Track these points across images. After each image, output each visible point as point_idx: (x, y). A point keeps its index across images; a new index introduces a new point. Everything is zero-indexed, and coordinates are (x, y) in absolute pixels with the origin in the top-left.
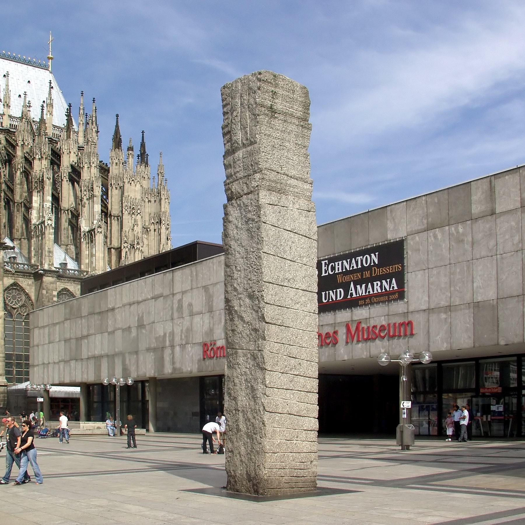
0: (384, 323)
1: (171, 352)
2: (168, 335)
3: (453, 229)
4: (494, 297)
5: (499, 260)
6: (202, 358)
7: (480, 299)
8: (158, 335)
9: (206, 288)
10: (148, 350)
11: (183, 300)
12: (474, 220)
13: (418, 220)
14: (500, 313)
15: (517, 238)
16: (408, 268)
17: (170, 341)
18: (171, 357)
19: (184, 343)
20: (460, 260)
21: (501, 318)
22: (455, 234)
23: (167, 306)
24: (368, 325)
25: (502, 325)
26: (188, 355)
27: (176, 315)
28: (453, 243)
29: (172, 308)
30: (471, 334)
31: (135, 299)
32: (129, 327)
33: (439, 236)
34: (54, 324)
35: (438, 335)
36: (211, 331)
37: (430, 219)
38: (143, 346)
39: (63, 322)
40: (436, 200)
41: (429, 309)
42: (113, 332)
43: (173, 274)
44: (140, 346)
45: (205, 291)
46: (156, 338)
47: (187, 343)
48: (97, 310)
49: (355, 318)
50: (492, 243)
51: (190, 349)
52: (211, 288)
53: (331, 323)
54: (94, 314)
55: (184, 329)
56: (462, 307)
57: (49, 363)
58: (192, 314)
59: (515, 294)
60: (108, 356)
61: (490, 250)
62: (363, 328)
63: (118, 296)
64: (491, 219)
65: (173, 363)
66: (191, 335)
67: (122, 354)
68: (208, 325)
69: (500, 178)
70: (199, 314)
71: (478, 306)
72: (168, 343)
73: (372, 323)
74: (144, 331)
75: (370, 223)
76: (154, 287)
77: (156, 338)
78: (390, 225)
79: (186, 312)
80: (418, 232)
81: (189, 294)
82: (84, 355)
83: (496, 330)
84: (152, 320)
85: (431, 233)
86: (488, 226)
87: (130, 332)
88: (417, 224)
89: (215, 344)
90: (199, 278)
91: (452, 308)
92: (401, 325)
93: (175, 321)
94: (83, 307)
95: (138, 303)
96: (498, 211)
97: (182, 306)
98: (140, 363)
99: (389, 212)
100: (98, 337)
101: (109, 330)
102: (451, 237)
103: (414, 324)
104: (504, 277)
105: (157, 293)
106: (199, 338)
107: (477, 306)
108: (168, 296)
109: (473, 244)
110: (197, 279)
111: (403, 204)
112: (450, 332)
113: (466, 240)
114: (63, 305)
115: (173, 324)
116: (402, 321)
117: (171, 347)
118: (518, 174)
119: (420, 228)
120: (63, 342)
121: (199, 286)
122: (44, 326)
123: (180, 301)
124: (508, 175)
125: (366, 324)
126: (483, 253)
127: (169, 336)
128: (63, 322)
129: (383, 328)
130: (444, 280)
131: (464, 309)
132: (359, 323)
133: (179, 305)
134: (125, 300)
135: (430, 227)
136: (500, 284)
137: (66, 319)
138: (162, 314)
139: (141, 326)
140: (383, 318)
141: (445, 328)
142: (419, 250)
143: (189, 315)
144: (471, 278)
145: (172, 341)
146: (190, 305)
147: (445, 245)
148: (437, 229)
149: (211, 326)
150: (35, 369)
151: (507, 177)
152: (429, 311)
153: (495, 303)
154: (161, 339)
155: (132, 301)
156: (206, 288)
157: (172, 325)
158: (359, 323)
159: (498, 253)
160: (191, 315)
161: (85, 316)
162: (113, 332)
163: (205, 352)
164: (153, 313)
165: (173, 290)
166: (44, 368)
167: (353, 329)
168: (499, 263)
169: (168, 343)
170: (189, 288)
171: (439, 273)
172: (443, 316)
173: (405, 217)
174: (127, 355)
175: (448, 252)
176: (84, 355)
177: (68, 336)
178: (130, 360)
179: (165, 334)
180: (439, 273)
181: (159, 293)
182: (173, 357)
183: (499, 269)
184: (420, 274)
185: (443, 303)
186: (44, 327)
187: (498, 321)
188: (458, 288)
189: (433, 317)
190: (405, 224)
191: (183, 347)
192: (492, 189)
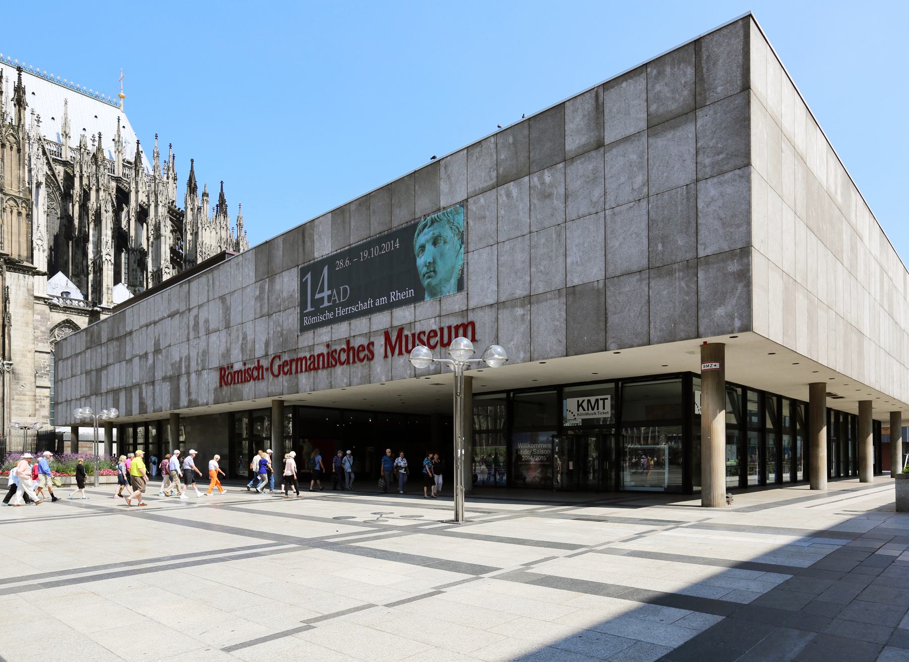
0: (434, 327)
1: (187, 381)
2: (184, 360)
3: (536, 179)
4: (601, 276)
5: (608, 217)
6: (218, 385)
7: (577, 281)
8: (174, 361)
9: (222, 298)
10: (164, 379)
12: (568, 160)
13: (483, 174)
14: (609, 301)
15: (639, 179)
16: (469, 245)
17: (185, 367)
18: (187, 387)
19: (200, 368)
20: (546, 224)
21: (611, 309)
22: (539, 187)
23: (183, 324)
24: (413, 332)
25: (613, 319)
26: (205, 384)
28: (535, 201)
29: (188, 328)
30: (562, 336)
31: (152, 319)
32: (146, 354)
34: (77, 355)
35: (511, 340)
37: (501, 170)
38: (159, 375)
39: (84, 351)
40: (511, 140)
41: (498, 303)
42: (131, 360)
45: (222, 302)
46: (172, 365)
47: (203, 369)
48: (116, 335)
49: (396, 323)
50: (597, 192)
51: (206, 376)
52: (228, 297)
54: (113, 339)
55: (201, 351)
56: (549, 296)
57: (72, 400)
58: (208, 333)
59: (635, 268)
61: (594, 204)
62: (407, 336)
63: (135, 317)
64: (597, 155)
65: (189, 394)
67: (138, 385)
68: (225, 344)
69: (612, 87)
71: (574, 293)
73: (418, 329)
74: (160, 357)
75: (416, 188)
77: (172, 365)
78: (444, 186)
80: (483, 191)
81: (205, 308)
82: (104, 390)
83: (603, 327)
85: (502, 190)
86: (591, 167)
87: (147, 359)
89: (232, 367)
90: (215, 287)
91: (533, 299)
93: (191, 342)
94: (103, 333)
95: (155, 323)
96: (607, 141)
97: (198, 323)
98: (156, 395)
99: (442, 169)
100: (117, 366)
101: (127, 358)
102: (532, 192)
103: (477, 326)
104: (617, 244)
105: (173, 309)
106: (215, 362)
107: (572, 293)
108: (183, 312)
110: (213, 287)
111: (462, 152)
113: (555, 193)
116: (459, 323)
118: (644, 75)
119: (485, 185)
120: (84, 375)
122: (67, 358)
123: (197, 317)
124: (626, 80)
125: (411, 331)
126: (583, 210)
127: (185, 361)
128: (84, 351)
130: (521, 257)
131: (551, 299)
132: (401, 330)
133: (195, 322)
134: (143, 322)
135: (501, 181)
136: (609, 256)
137: (87, 349)
139: (157, 351)
140: (433, 320)
141: (522, 329)
142: (484, 217)
143: (205, 334)
144: (562, 250)
145: (188, 367)
146: (207, 321)
147: (523, 206)
148: (512, 183)
149: (228, 346)
150: (59, 406)
151: (624, 84)
152: (498, 305)
153: (601, 285)
156: (222, 298)
158: (401, 330)
159: (607, 207)
161: (104, 343)
162: (131, 360)
163: (222, 378)
165: (189, 305)
166: (67, 405)
167: (394, 339)
168: (608, 222)
171: (513, 249)
172: (519, 311)
173: (465, 171)
174: (144, 386)
175: (527, 215)
176: (104, 390)
177: (88, 368)
178: (147, 391)
180: (513, 249)
182: (189, 386)
183: (608, 232)
184: (485, 253)
185: (520, 292)
186: (67, 358)
187: (606, 314)
188: (542, 268)
189: (505, 314)
190: (465, 183)
192: (599, 108)
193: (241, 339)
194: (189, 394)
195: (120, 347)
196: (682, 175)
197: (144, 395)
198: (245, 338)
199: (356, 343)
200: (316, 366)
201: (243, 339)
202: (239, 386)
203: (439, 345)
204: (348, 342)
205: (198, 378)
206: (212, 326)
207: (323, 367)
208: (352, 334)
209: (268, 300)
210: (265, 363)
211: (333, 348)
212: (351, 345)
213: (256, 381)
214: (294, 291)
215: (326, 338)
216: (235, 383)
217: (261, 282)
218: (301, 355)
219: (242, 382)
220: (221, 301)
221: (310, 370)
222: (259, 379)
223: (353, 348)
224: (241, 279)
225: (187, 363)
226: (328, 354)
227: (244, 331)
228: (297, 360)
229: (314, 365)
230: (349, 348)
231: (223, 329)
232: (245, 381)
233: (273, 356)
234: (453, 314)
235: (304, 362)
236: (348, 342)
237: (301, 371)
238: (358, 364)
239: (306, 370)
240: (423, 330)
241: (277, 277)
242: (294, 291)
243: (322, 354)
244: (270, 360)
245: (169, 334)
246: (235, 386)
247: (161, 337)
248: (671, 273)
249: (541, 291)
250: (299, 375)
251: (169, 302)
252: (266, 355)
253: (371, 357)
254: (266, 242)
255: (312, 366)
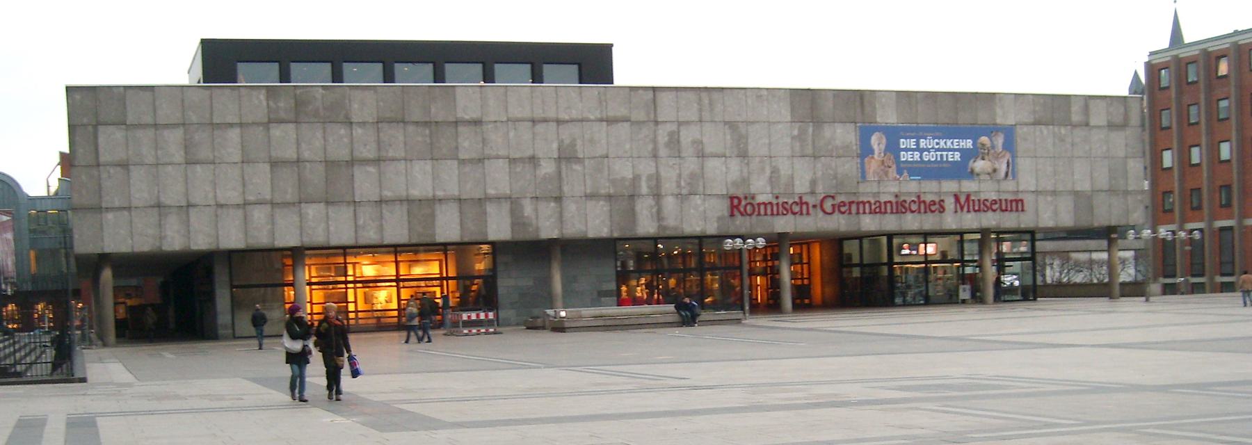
0: (994, 198)
4: (1089, 189)
6: (726, 213)
7: (1079, 189)
8: (618, 177)
9: (732, 125)
11: (681, 133)
12: (1074, 126)
15: (1105, 148)
17: (649, 187)
18: (654, 210)
19: (684, 192)
27: (663, 152)
29: (655, 141)
31: (551, 114)
32: (533, 160)
33: (1045, 132)
36: (745, 181)
37: (1037, 116)
43: (654, 96)
44: (566, 188)
45: (730, 127)
46: (613, 182)
49: (964, 190)
50: (1087, 148)
51: (699, 202)
53: (935, 191)
55: (686, 173)
60: (460, 200)
62: (973, 200)
65: (659, 216)
66: (701, 184)
70: (719, 157)
72: (644, 189)
73: (983, 197)
74: (577, 167)
76: (604, 104)
78: (999, 111)
79: (688, 150)
80: (1026, 124)
84: (600, 151)
85: (1038, 127)
88: (1026, 117)
89: (753, 198)
92: (1011, 201)
95: (559, 122)
96: (1092, 123)
97: (679, 142)
98: (567, 215)
101: (462, 156)
103: (1025, 201)
107: (1076, 194)
108: (639, 123)
109: (1073, 145)
110: (712, 110)
112: (1056, 213)
114: (264, 91)
115: (657, 165)
116: (1013, 198)
117: (654, 196)
119: (1027, 121)
121: (717, 120)
125: (975, 196)
129: (995, 202)
138: (628, 146)
139: (567, 156)
146: (698, 144)
149: (746, 175)
152: (1036, 192)
154: (627, 183)
155: (538, 114)
156: (732, 125)
157: (654, 165)
160: (701, 155)
164: (603, 141)
165: (655, 116)
167: (963, 199)
169: (644, 189)
170: (695, 118)
172: (1049, 199)
177: (291, 154)
179: (636, 179)
181: (619, 114)
182: (659, 212)
185: (1049, 188)
189: (1041, 198)
191: (680, 197)
193: (768, 171)
194: (659, 216)
195: (431, 136)
196: (1122, 154)
197: (528, 209)
198: (775, 171)
199: (928, 198)
200: (883, 210)
201: (772, 172)
202: (768, 218)
203: (999, 210)
204: (919, 197)
205: (682, 203)
206: (709, 149)
207: (892, 213)
208: (923, 191)
209: (814, 142)
210: (811, 200)
211: (902, 198)
212: (922, 199)
213: (797, 216)
214: (851, 142)
215: (895, 190)
216: (759, 214)
217: (801, 124)
218: (865, 200)
219: (772, 214)
220: (727, 127)
221: (876, 213)
222: (802, 214)
223: (924, 202)
224: (765, 113)
225: (654, 183)
226: (897, 203)
227: (774, 164)
228: (858, 203)
229: (880, 209)
230: (920, 202)
231: (733, 155)
232: (778, 214)
233: (823, 195)
234: (1008, 192)
235: (867, 205)
236: (919, 197)
237: (864, 213)
238: (929, 214)
239: (870, 213)
240: (986, 198)
241: (826, 127)
242: (851, 142)
243: (890, 202)
244: (821, 197)
245: (604, 142)
246: (760, 218)
247: (579, 142)
248: (1118, 195)
249: (1061, 189)
250: (862, 217)
251: (600, 102)
252: (813, 193)
253: (942, 209)
254: (809, 89)
255: (877, 210)
